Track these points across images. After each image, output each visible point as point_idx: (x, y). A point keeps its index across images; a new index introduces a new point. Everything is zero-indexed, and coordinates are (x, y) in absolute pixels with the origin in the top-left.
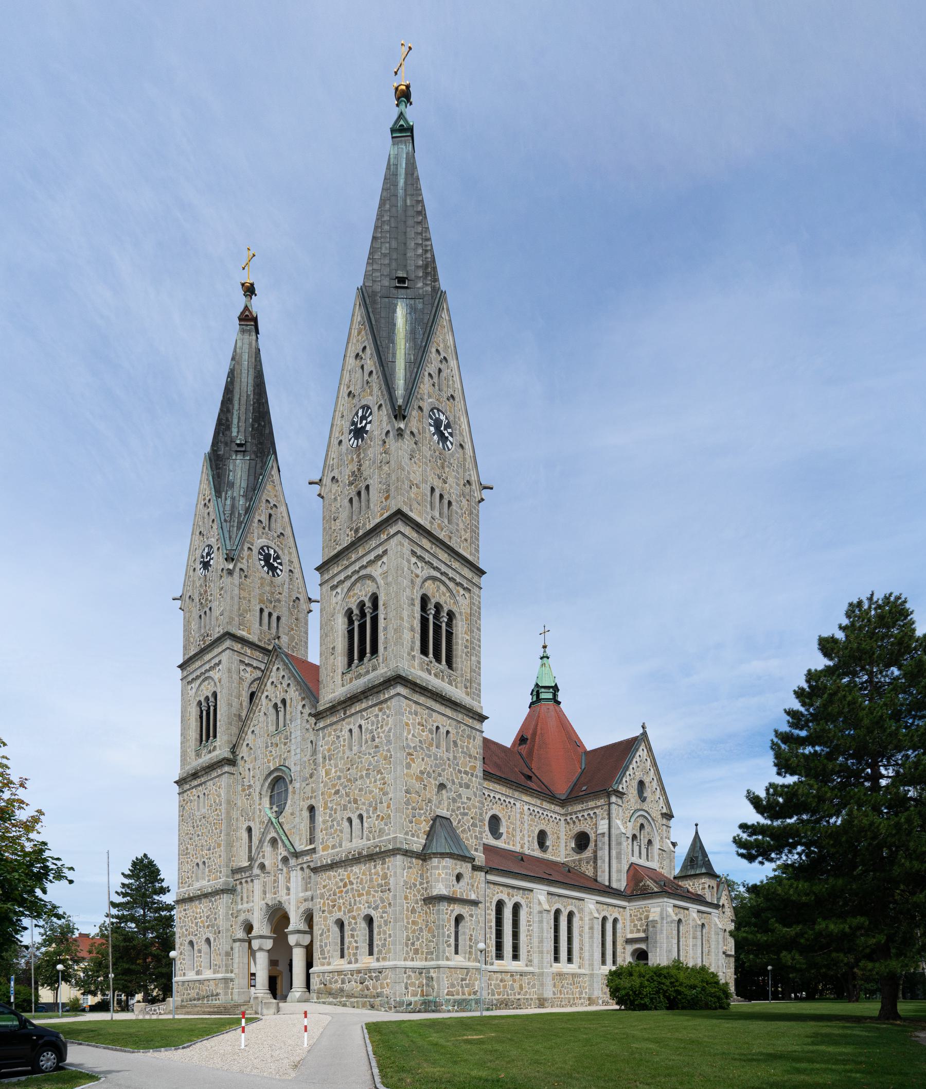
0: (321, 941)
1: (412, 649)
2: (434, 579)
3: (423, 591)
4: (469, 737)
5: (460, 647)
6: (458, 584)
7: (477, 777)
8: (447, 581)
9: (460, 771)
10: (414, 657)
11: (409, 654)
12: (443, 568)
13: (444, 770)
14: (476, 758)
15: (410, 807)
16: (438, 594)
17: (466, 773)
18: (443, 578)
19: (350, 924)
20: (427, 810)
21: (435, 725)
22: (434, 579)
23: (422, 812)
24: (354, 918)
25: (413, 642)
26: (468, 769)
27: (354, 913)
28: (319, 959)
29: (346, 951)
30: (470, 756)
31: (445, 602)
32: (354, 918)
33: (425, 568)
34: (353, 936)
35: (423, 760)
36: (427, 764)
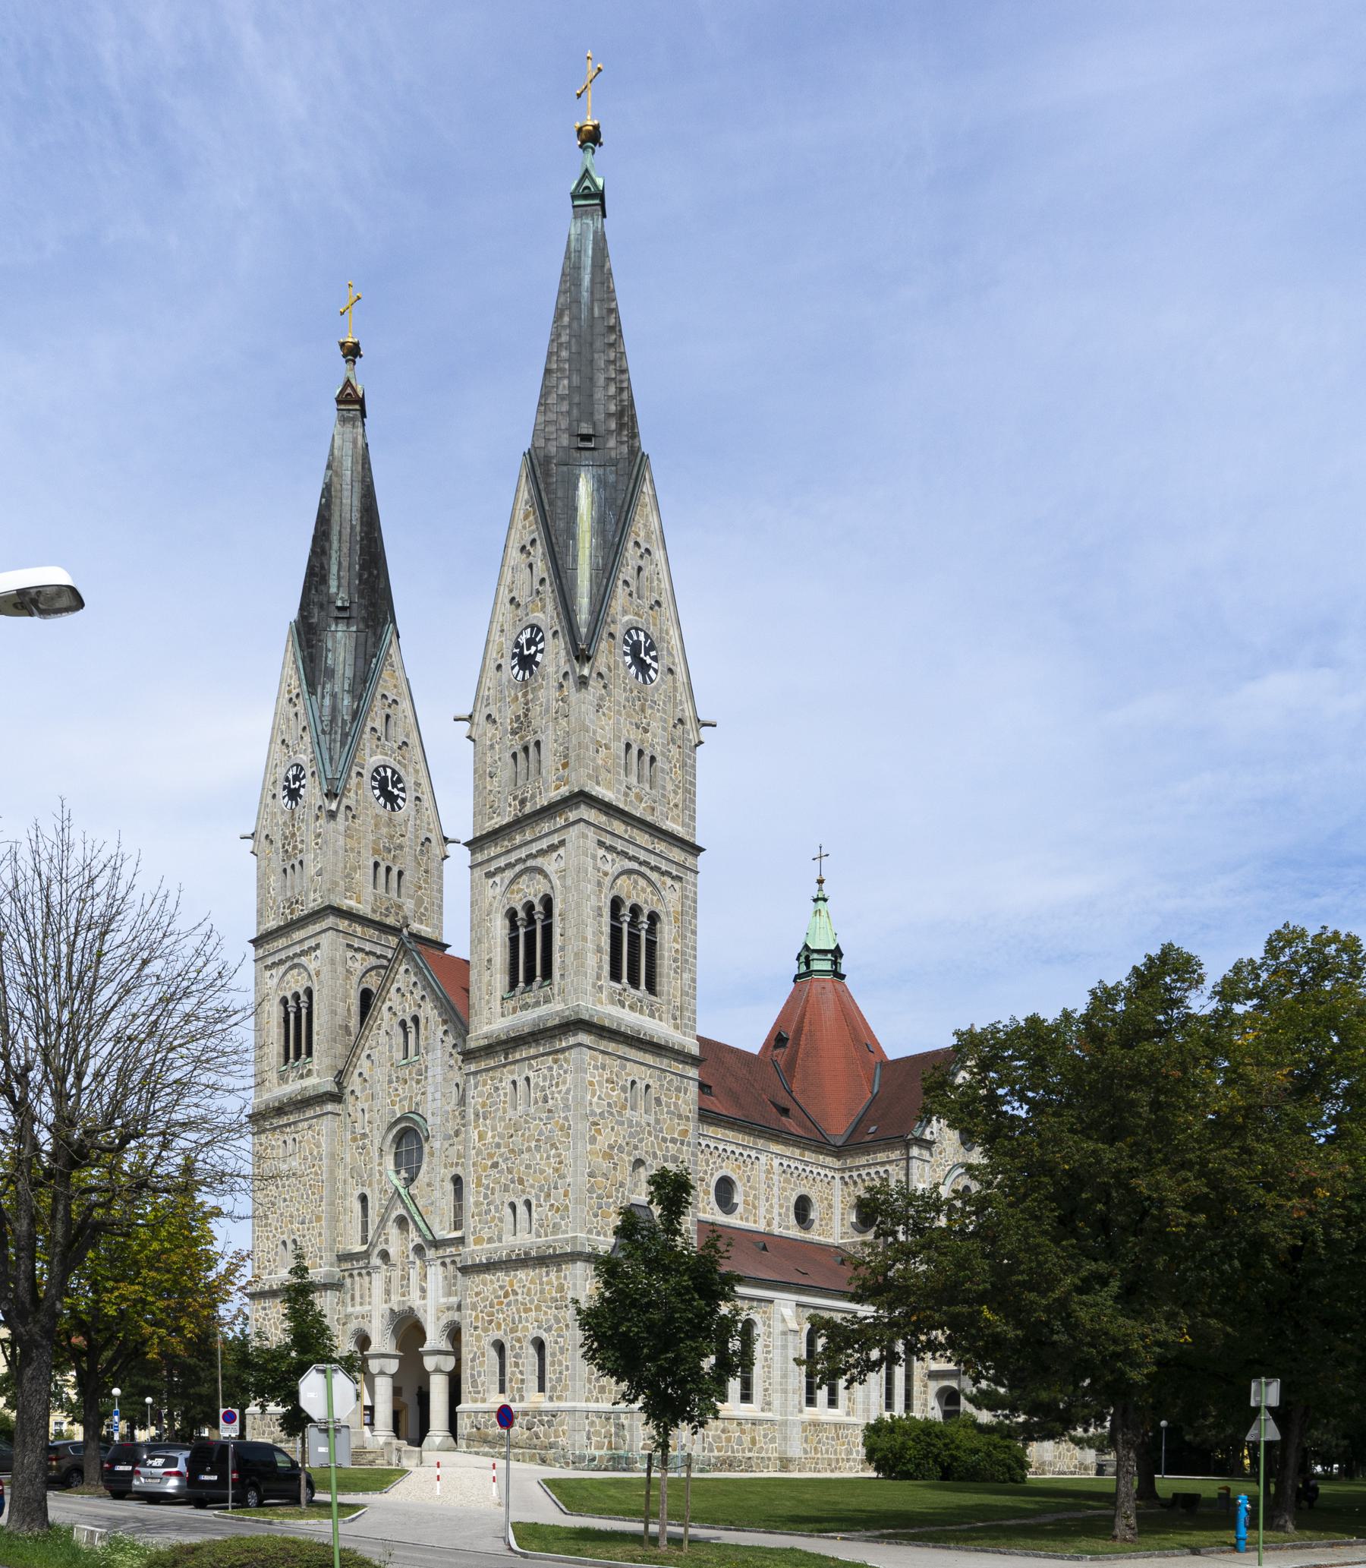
0: (473, 1368)
1: (599, 978)
2: (629, 872)
3: (614, 892)
4: (678, 1089)
5: (666, 962)
6: (664, 873)
7: (689, 1144)
8: (648, 872)
9: (664, 1140)
10: (601, 988)
11: (594, 985)
12: (642, 856)
13: (641, 1141)
14: (687, 1118)
15: (595, 1196)
16: (635, 892)
17: (673, 1141)
18: (643, 869)
19: (513, 1348)
20: (617, 1198)
21: (630, 1079)
22: (629, 872)
23: (611, 1200)
24: (519, 1340)
25: (600, 968)
26: (676, 1136)
27: (519, 1334)
28: (470, 1392)
29: (507, 1385)
30: (680, 1117)
31: (646, 902)
32: (519, 1340)
33: (617, 860)
34: (517, 1365)
35: (613, 1129)
36: (618, 1135)
